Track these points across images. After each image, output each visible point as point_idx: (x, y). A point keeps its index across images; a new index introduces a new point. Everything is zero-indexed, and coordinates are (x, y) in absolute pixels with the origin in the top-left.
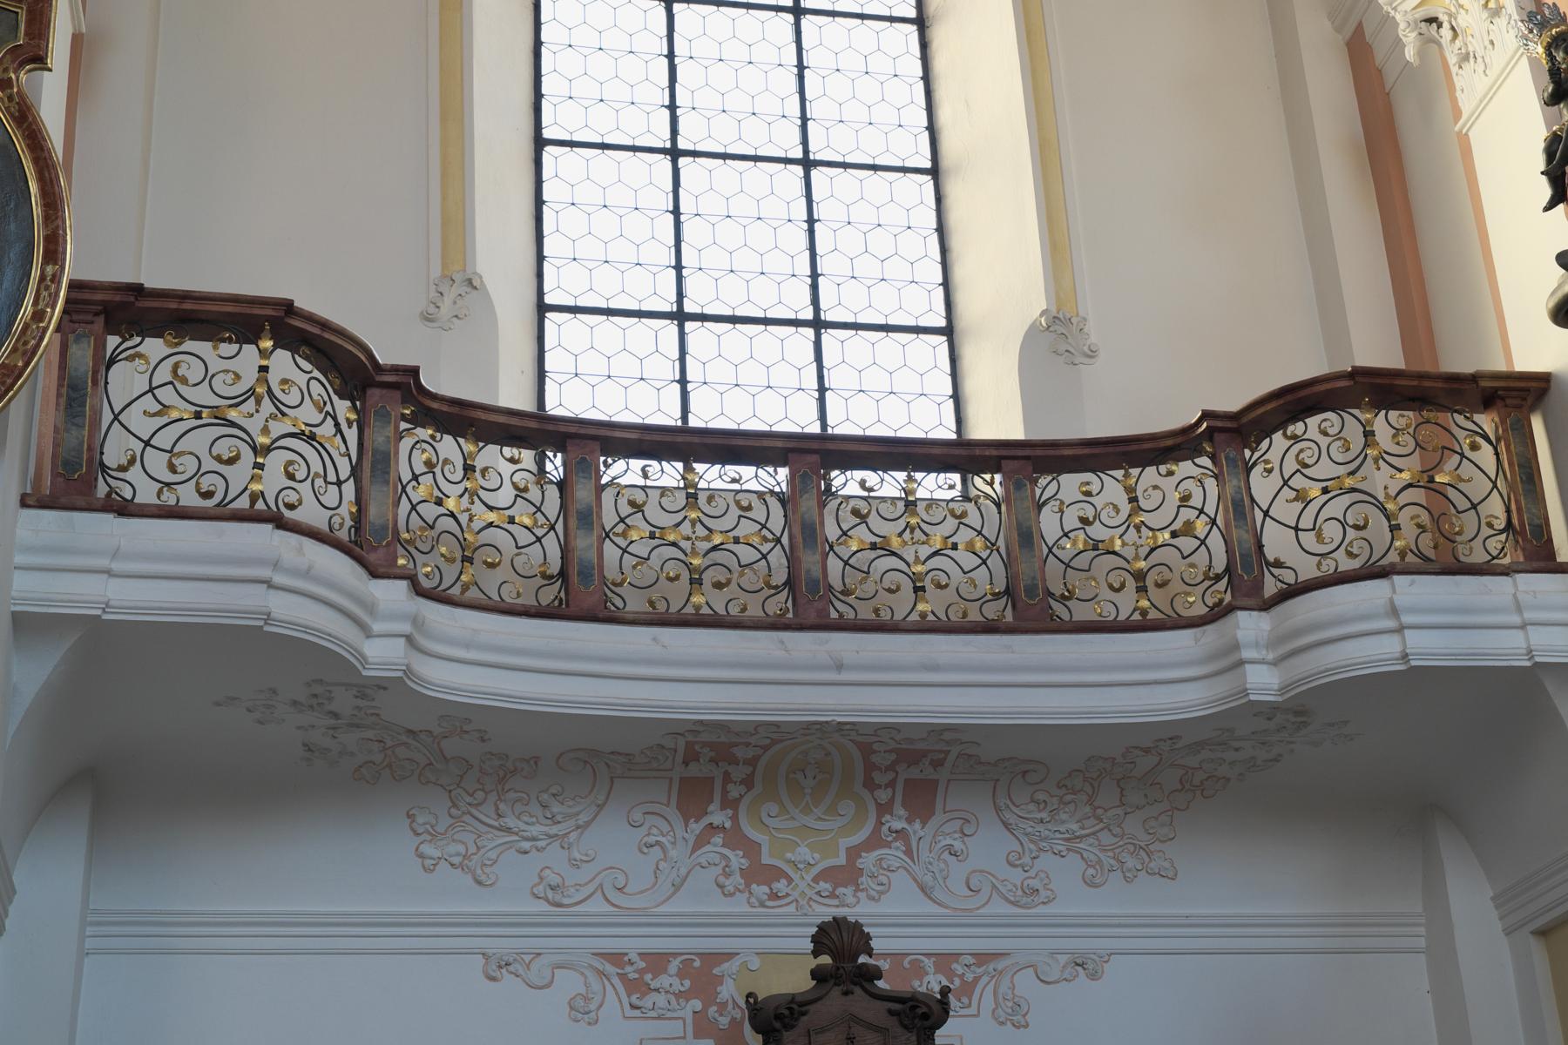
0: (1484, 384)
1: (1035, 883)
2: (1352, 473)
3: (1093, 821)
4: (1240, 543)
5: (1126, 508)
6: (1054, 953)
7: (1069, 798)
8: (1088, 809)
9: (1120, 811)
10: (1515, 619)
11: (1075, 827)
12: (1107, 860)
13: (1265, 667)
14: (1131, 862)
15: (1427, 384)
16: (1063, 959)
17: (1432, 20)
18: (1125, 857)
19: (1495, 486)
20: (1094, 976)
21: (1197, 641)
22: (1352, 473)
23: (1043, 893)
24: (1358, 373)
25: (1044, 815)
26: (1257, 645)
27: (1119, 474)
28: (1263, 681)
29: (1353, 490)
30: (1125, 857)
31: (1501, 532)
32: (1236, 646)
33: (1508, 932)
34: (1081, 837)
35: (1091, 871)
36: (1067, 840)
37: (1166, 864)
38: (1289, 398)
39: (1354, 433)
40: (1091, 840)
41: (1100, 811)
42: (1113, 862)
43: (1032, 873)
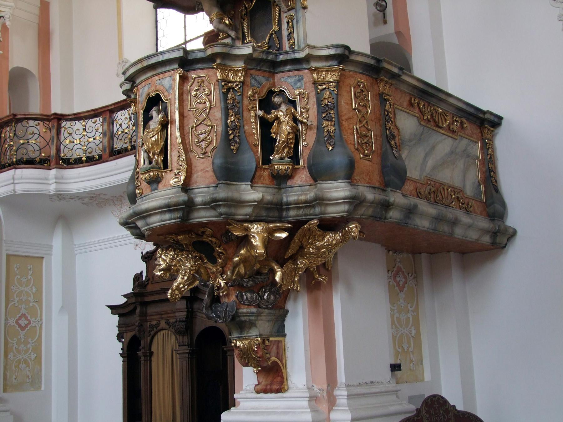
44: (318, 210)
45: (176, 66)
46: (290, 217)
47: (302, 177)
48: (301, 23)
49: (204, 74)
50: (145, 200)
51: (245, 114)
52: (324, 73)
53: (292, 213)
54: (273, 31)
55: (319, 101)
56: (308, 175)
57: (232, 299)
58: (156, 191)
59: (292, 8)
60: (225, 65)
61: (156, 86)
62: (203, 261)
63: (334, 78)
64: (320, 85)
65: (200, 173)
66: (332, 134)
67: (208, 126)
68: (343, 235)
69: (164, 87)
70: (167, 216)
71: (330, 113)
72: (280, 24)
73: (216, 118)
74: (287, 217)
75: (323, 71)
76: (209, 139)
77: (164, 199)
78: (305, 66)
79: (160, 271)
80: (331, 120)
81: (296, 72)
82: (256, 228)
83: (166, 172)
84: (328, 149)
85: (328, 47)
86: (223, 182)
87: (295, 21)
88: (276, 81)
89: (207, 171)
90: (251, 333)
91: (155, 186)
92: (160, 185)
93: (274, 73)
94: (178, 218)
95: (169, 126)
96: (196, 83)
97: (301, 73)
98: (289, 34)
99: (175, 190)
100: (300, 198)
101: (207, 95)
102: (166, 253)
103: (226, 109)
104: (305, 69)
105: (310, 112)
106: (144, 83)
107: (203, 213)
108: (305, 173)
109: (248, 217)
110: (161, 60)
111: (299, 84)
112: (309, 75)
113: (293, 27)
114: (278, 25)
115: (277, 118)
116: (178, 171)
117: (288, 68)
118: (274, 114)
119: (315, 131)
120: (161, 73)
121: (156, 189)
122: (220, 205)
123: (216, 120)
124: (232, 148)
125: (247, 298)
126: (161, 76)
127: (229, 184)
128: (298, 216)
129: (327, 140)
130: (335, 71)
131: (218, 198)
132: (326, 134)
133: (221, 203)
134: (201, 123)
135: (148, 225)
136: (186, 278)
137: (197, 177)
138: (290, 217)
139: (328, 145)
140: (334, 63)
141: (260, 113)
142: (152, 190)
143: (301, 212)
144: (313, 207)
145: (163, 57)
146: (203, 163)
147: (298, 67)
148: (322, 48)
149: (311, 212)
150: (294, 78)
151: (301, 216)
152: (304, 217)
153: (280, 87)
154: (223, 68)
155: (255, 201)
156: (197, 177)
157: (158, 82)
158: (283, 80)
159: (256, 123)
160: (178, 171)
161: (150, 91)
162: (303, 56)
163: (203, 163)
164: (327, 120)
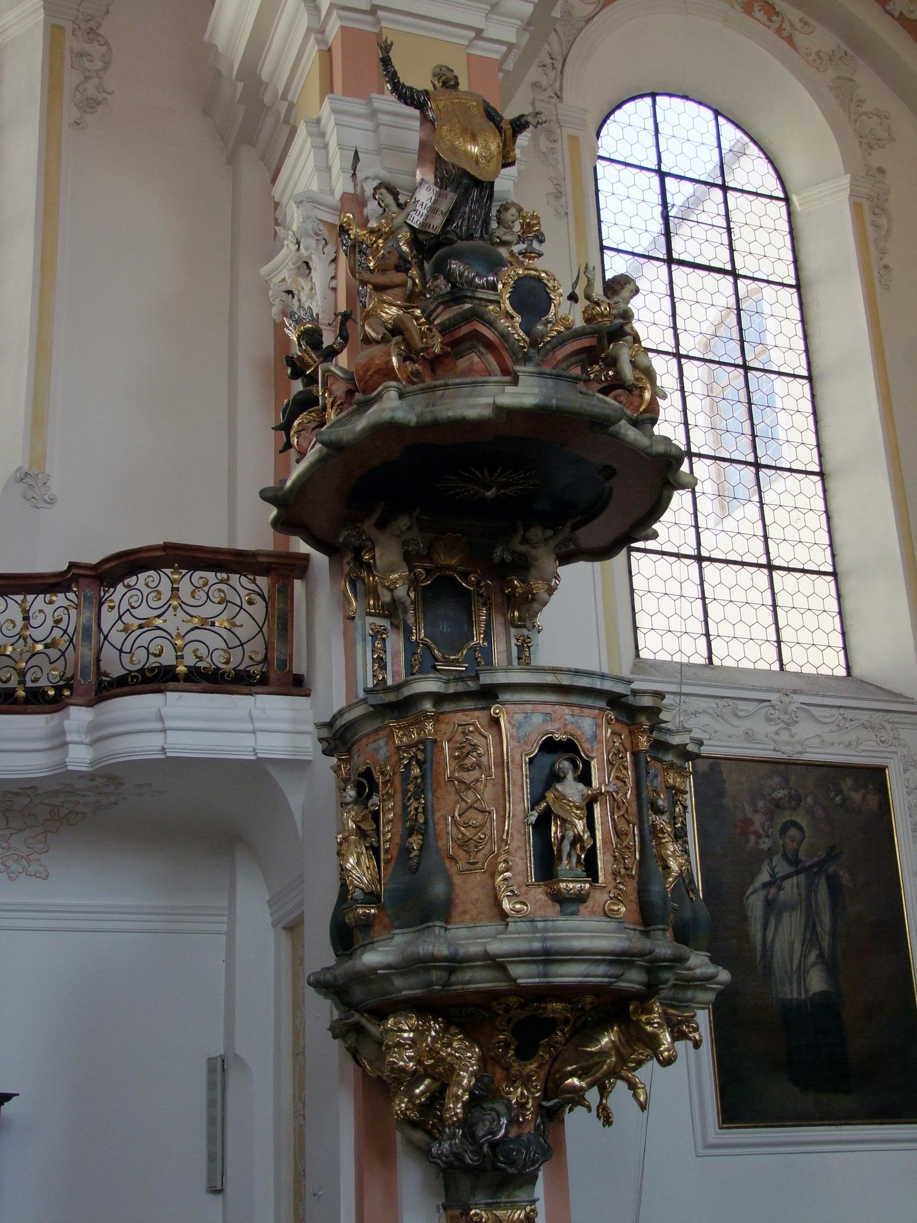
0: (260, 559)
2: (159, 616)
4: (82, 657)
5: (20, 623)
9: (6, 832)
10: (250, 727)
13: (84, 746)
14: (14, 867)
15: (219, 557)
17: (289, 292)
18: (10, 863)
19: (261, 630)
21: (47, 723)
22: (159, 616)
24: (167, 547)
26: (78, 732)
27: (19, 598)
28: (80, 757)
29: (159, 628)
30: (10, 863)
31: (259, 663)
32: (62, 732)
33: (274, 925)
37: (41, 869)
38: (124, 559)
39: (165, 588)
45: (603, 704)
57: (526, 1131)
61: (566, 725)
70: (601, 969)
72: (488, 637)
91: (573, 908)
92: (582, 908)
106: (529, 707)
114: (484, 639)
126: (577, 710)
135: (546, 975)
142: (562, 913)
145: (602, 684)
157: (569, 718)
161: (549, 728)
162: (674, 743)
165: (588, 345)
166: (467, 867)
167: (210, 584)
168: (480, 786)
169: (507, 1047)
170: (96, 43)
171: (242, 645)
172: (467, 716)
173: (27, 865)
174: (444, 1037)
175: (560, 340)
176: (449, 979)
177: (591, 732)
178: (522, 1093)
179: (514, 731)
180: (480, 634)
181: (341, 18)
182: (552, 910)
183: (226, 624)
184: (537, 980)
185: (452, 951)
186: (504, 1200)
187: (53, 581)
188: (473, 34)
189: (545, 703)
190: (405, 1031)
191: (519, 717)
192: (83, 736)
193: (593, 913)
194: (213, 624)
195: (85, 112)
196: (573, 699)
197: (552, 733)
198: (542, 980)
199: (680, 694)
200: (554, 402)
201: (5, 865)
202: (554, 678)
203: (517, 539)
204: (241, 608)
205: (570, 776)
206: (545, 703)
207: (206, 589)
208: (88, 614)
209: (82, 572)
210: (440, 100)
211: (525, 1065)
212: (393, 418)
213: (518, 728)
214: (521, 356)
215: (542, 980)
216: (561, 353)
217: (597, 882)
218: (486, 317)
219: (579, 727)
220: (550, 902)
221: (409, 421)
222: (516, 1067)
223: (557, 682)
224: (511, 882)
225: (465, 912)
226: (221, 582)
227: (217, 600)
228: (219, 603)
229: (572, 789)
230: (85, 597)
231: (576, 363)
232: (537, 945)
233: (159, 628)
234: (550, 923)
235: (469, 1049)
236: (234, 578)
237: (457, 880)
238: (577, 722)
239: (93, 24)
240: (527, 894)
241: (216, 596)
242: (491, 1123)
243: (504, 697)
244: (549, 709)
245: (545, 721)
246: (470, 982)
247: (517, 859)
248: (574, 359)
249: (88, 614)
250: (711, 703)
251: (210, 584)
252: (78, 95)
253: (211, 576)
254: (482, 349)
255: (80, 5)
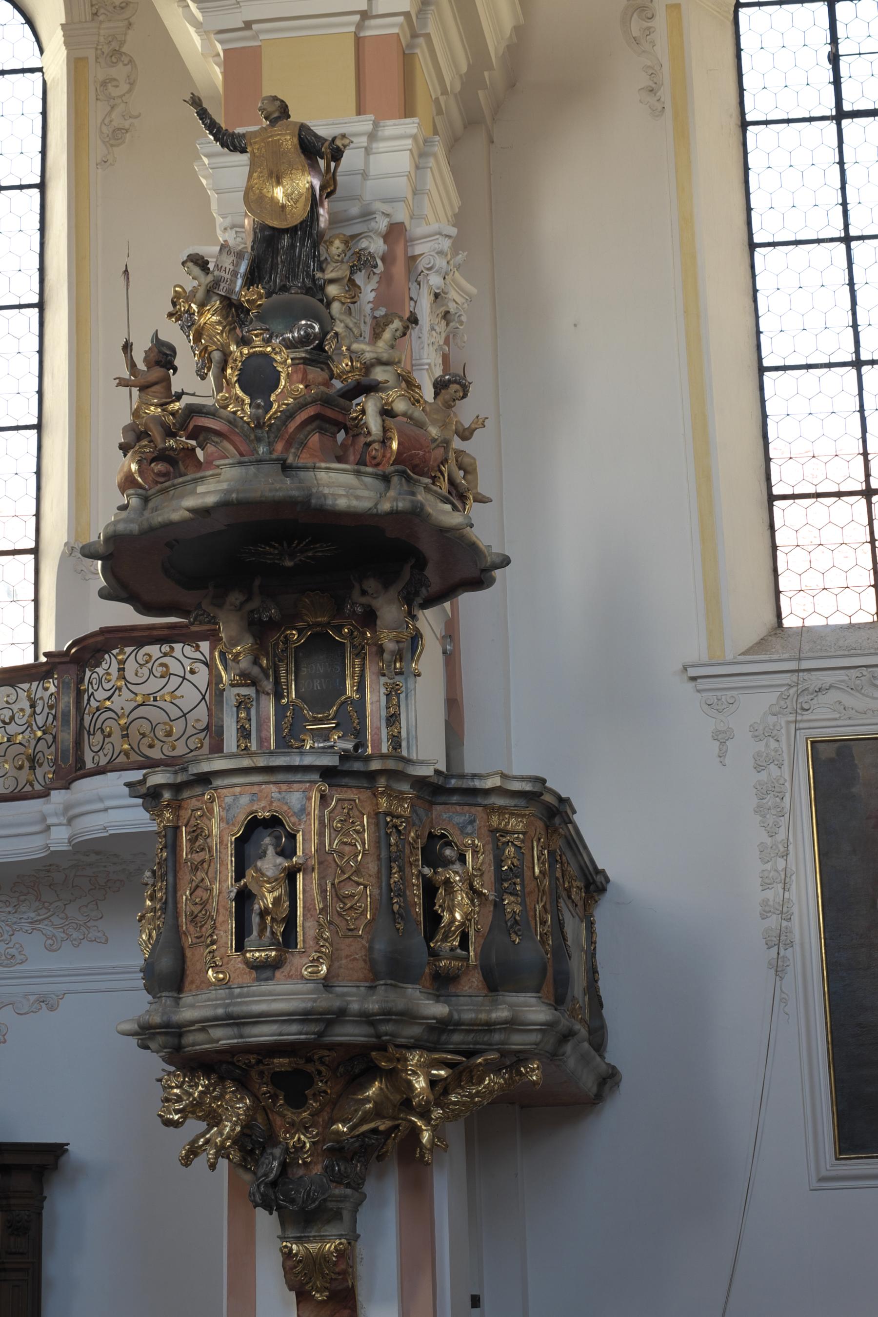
1: (13, 951)
2: (109, 699)
3: (44, 911)
4: (62, 742)
5: (28, 711)
6: (26, 995)
7: (22, 898)
8: (37, 903)
9: (59, 904)
11: (32, 915)
12: (60, 934)
13: (64, 827)
14: (75, 935)
16: (32, 998)
19: (204, 698)
20: (52, 1008)
22: (109, 699)
23: (19, 958)
24: (104, 631)
25: (9, 909)
26: (56, 814)
27: (25, 686)
31: (203, 730)
34: (40, 921)
35: (50, 942)
36: (31, 923)
37: (99, 935)
40: (46, 922)
41: (46, 905)
42: (63, 935)
43: (11, 945)
44: (497, 1037)
45: (316, 777)
46: (452, 1044)
47: (473, 982)
48: (412, 701)
49: (352, 796)
50: (240, 996)
51: (407, 870)
52: (507, 816)
53: (457, 1038)
54: (350, 697)
55: (498, 862)
56: (481, 978)
57: (314, 1172)
58: (271, 983)
59: (401, 673)
60: (392, 789)
61: (272, 802)
62: (274, 1103)
63: (520, 827)
64: (501, 836)
65: (344, 961)
66: (518, 918)
67: (359, 884)
68: (511, 1078)
69: (289, 808)
70: (294, 1028)
71: (515, 884)
72: (361, 688)
73: (371, 873)
74: (446, 1044)
75: (505, 813)
76: (360, 907)
77: (303, 1000)
78: (480, 800)
79: (177, 1112)
80: (517, 895)
81: (466, 808)
82: (415, 1058)
83: (292, 954)
84: (514, 941)
85: (522, 779)
86: (389, 982)
87: (402, 696)
88: (434, 817)
89: (355, 959)
90: (326, 1231)
91: (268, 973)
92: (278, 974)
93: (432, 803)
94: (314, 1033)
95: (300, 877)
96: (339, 808)
97: (474, 810)
98: (391, 716)
99: (310, 986)
100: (480, 1016)
101: (358, 832)
102: (191, 1080)
103: (390, 860)
104: (479, 805)
105: (485, 877)
106: (238, 789)
107: (350, 1029)
108: (477, 975)
109: (412, 1040)
110: (297, 764)
111: (469, 829)
112: (485, 817)
113: (399, 707)
114: (357, 691)
115: (447, 882)
116: (319, 955)
117: (455, 799)
118: (444, 873)
119: (492, 909)
120: (284, 782)
121: (267, 979)
122: (388, 1021)
123: (370, 876)
124: (398, 926)
125: (339, 1170)
126: (284, 787)
127: (395, 986)
128: (463, 1043)
129: (512, 927)
130: (524, 816)
131: (394, 1009)
132: (509, 916)
133: (394, 1017)
134: (349, 878)
135: (242, 1037)
136: (238, 1129)
137: (340, 967)
138: (452, 1044)
139: (514, 936)
140: (522, 802)
141: (427, 871)
142: (258, 979)
143: (470, 1037)
144: (490, 1031)
145: (301, 760)
146: (350, 946)
147: (470, 800)
148: (515, 778)
149: (486, 1039)
150: (463, 818)
151: (469, 1043)
152: (471, 1046)
153: (444, 829)
154: (389, 793)
155: (434, 1018)
156: (340, 967)
158: (445, 816)
159: (418, 886)
160: (319, 955)
161: (255, 808)
162: (487, 787)
163: (350, 946)
164: (511, 894)
165: (312, 414)
166: (195, 941)
167: (154, 659)
168: (205, 865)
169: (274, 1097)
170: (121, 64)
171: (185, 715)
172: (198, 801)
173: (87, 932)
174: (214, 1090)
175: (288, 414)
176: (180, 1042)
177: (299, 806)
178: (299, 1139)
179: (223, 814)
180: (354, 686)
181: (221, 42)
182: (248, 977)
183: (168, 698)
184: (236, 1041)
185: (165, 1018)
186: (313, 1234)
187: (166, 632)
188: (357, 18)
189: (252, 784)
190: (173, 1088)
191: (229, 800)
192: (62, 818)
193: (289, 977)
194: (155, 700)
195: (112, 146)
196: (281, 777)
197: (256, 812)
198: (240, 1040)
199: (798, 671)
200: (234, 496)
201: (67, 934)
202: (251, 762)
203: (356, 593)
204: (184, 678)
205: (271, 851)
206: (252, 784)
207: (149, 665)
208: (66, 699)
209: (57, 660)
210: (255, 143)
211: (301, 1113)
212: (115, 531)
213: (228, 811)
214: (252, 437)
215: (240, 1040)
216: (292, 426)
217: (296, 947)
218: (205, 411)
219: (287, 803)
220: (248, 970)
221: (131, 531)
222: (289, 1114)
223: (253, 765)
224: (216, 953)
225: (192, 982)
226: (165, 655)
227: (158, 675)
228: (162, 677)
229: (271, 864)
230: (63, 682)
231: (313, 430)
232: (220, 1011)
233: (110, 709)
234: (246, 989)
235: (241, 1100)
236: (178, 646)
237: (188, 953)
238: (284, 798)
239: (115, 45)
240: (228, 964)
241: (158, 671)
242: (267, 1166)
243: (218, 782)
244: (256, 789)
245: (252, 801)
246: (194, 1045)
247: (222, 933)
248: (309, 428)
249: (66, 699)
250: (841, 675)
251: (154, 659)
252: (105, 129)
253: (154, 650)
254: (216, 439)
255: (99, 28)
